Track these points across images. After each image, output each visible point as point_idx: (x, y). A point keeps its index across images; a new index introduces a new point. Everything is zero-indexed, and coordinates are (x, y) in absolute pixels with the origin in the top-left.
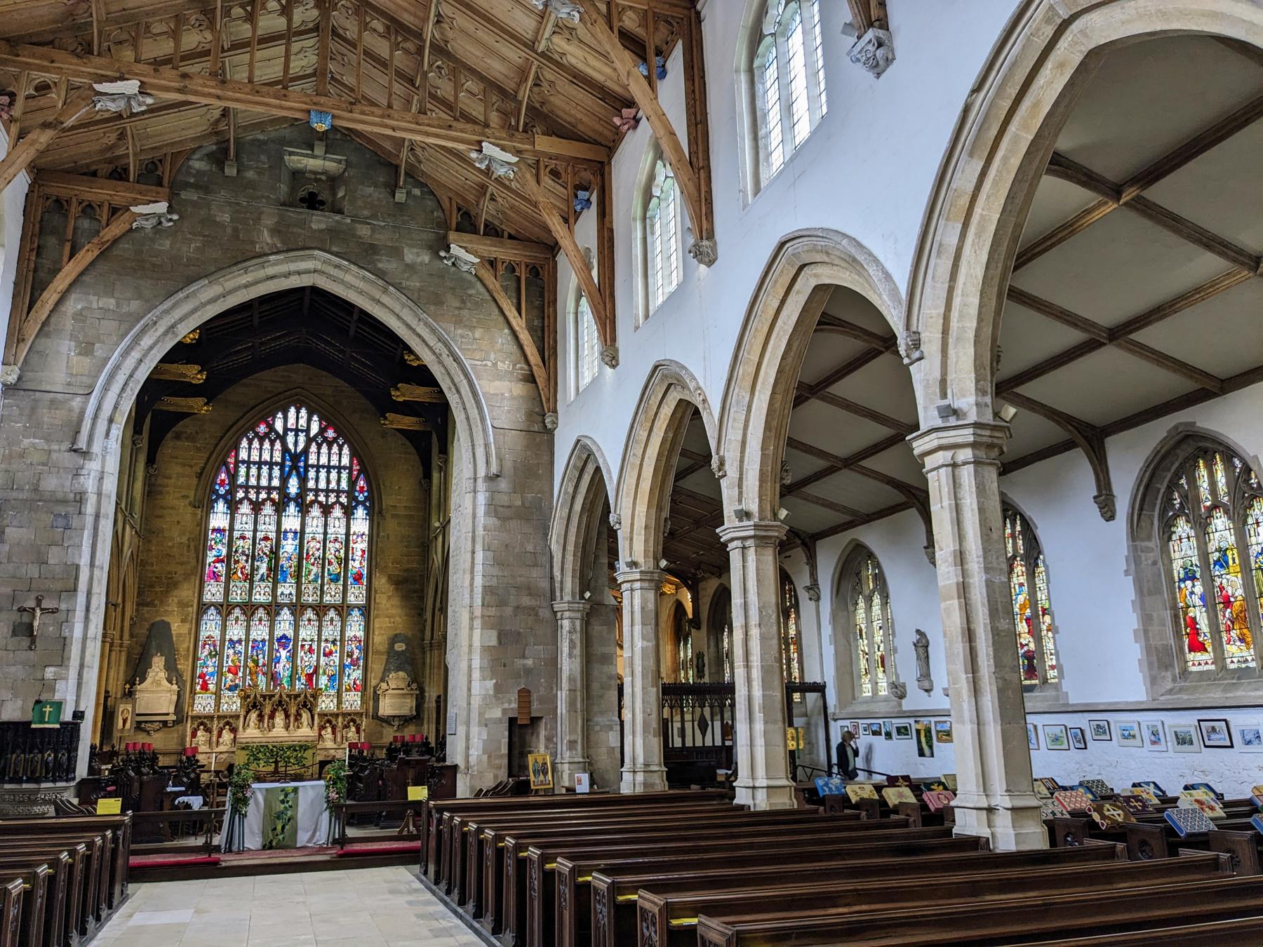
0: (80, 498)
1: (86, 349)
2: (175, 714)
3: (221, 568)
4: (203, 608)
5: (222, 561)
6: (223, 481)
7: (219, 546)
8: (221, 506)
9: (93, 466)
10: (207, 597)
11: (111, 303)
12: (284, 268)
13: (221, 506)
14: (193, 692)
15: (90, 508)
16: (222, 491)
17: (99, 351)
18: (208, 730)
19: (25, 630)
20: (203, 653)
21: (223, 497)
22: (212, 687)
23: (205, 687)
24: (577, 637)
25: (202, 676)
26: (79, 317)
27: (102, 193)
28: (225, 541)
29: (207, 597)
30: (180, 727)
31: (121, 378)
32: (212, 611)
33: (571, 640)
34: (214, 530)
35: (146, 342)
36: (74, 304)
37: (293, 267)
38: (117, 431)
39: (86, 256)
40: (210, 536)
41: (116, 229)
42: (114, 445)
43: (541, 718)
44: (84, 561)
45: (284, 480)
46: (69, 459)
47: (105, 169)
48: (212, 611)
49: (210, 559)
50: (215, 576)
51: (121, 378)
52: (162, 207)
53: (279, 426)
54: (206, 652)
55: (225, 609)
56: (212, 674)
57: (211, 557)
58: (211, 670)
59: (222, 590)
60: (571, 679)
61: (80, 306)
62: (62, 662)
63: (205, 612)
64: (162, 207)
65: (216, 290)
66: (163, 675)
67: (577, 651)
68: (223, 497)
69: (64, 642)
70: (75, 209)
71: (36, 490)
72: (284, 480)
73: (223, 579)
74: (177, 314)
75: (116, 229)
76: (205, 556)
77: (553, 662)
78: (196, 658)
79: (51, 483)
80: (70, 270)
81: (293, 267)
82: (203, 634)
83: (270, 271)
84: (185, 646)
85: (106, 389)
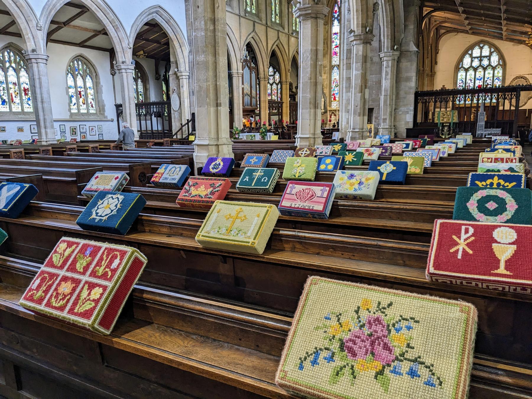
2: (324, 109)
3: (337, 50)
4: (332, 67)
5: (338, 47)
6: (336, 11)
7: (336, 41)
8: (336, 23)
10: (334, 63)
13: (336, 23)
14: (330, 102)
16: (336, 16)
18: (335, 115)
20: (333, 86)
21: (337, 18)
22: (337, 99)
23: (335, 99)
24: (389, 70)
25: (334, 94)
28: (338, 38)
29: (334, 63)
30: (325, 114)
32: (335, 68)
33: (386, 72)
34: (334, 34)
40: (333, 37)
43: (373, 109)
48: (335, 68)
49: (333, 46)
50: (336, 53)
54: (334, 85)
56: (337, 94)
57: (334, 45)
58: (336, 92)
59: (338, 59)
60: (386, 90)
63: (333, 69)
67: (389, 77)
68: (337, 18)
73: (338, 54)
76: (331, 46)
77: (380, 82)
78: (330, 88)
82: (333, 78)
84: (326, 83)
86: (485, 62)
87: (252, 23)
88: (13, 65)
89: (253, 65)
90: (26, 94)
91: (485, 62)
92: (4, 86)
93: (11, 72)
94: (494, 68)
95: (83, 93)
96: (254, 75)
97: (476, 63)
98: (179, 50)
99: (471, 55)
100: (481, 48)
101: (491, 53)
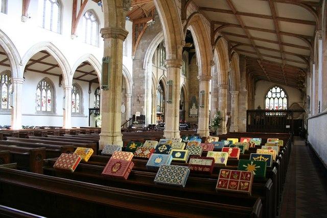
11: (146, 41)
15: (146, 79)
19: (138, 100)
26: (142, 45)
27: (142, 21)
35: (152, 47)
36: (141, 43)
39: (142, 33)
41: (145, 27)
44: (146, 88)
47: (143, 16)
52: (152, 21)
62: (144, 106)
64: (152, 21)
70: (139, 25)
75: (145, 27)
79: (140, 75)
80: (140, 36)
85: (147, 57)
86: (278, 95)
87: (162, 71)
88: (45, 88)
89: (162, 91)
90: (49, 102)
91: (278, 95)
92: (40, 98)
93: (44, 91)
94: (283, 99)
95: (74, 102)
96: (162, 96)
97: (274, 96)
98: (128, 84)
99: (271, 92)
100: (276, 89)
101: (281, 91)
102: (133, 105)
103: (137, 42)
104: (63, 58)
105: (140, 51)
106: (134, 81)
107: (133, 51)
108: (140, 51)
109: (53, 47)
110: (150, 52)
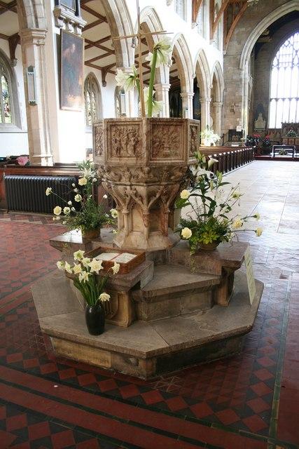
0: (241, 80)
1: (239, 43)
9: (243, 72)
12: (286, 8)
15: (243, 82)
17: (243, 43)
26: (237, 34)
31: (248, 49)
35: (253, 38)
36: (236, 32)
37: (290, 6)
38: (247, 63)
39: (238, 18)
42: (247, 66)
45: (293, 59)
46: (237, 71)
51: (248, 49)
53: (292, 43)
55: (277, 100)
61: (237, 31)
62: (240, 117)
65: (269, 19)
66: (261, 118)
69: (240, 113)
71: (232, 79)
72: (293, 59)
74: (259, 29)
75: (244, 9)
79: (235, 77)
80: (235, 23)
81: (290, 6)
83: (283, 9)
85: (245, 52)
98: (219, 88)
102: (224, 116)
103: (231, 31)
104: (189, 57)
105: (235, 43)
106: (225, 84)
107: (225, 43)
108: (235, 43)
109: (183, 41)
110: (249, 44)
